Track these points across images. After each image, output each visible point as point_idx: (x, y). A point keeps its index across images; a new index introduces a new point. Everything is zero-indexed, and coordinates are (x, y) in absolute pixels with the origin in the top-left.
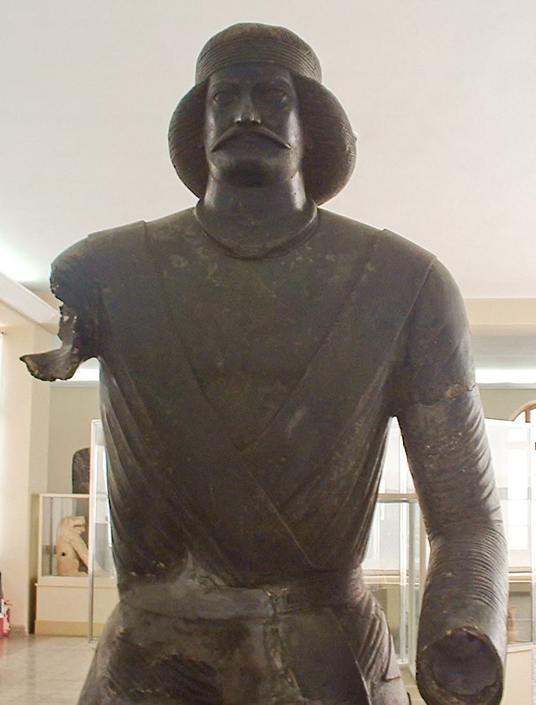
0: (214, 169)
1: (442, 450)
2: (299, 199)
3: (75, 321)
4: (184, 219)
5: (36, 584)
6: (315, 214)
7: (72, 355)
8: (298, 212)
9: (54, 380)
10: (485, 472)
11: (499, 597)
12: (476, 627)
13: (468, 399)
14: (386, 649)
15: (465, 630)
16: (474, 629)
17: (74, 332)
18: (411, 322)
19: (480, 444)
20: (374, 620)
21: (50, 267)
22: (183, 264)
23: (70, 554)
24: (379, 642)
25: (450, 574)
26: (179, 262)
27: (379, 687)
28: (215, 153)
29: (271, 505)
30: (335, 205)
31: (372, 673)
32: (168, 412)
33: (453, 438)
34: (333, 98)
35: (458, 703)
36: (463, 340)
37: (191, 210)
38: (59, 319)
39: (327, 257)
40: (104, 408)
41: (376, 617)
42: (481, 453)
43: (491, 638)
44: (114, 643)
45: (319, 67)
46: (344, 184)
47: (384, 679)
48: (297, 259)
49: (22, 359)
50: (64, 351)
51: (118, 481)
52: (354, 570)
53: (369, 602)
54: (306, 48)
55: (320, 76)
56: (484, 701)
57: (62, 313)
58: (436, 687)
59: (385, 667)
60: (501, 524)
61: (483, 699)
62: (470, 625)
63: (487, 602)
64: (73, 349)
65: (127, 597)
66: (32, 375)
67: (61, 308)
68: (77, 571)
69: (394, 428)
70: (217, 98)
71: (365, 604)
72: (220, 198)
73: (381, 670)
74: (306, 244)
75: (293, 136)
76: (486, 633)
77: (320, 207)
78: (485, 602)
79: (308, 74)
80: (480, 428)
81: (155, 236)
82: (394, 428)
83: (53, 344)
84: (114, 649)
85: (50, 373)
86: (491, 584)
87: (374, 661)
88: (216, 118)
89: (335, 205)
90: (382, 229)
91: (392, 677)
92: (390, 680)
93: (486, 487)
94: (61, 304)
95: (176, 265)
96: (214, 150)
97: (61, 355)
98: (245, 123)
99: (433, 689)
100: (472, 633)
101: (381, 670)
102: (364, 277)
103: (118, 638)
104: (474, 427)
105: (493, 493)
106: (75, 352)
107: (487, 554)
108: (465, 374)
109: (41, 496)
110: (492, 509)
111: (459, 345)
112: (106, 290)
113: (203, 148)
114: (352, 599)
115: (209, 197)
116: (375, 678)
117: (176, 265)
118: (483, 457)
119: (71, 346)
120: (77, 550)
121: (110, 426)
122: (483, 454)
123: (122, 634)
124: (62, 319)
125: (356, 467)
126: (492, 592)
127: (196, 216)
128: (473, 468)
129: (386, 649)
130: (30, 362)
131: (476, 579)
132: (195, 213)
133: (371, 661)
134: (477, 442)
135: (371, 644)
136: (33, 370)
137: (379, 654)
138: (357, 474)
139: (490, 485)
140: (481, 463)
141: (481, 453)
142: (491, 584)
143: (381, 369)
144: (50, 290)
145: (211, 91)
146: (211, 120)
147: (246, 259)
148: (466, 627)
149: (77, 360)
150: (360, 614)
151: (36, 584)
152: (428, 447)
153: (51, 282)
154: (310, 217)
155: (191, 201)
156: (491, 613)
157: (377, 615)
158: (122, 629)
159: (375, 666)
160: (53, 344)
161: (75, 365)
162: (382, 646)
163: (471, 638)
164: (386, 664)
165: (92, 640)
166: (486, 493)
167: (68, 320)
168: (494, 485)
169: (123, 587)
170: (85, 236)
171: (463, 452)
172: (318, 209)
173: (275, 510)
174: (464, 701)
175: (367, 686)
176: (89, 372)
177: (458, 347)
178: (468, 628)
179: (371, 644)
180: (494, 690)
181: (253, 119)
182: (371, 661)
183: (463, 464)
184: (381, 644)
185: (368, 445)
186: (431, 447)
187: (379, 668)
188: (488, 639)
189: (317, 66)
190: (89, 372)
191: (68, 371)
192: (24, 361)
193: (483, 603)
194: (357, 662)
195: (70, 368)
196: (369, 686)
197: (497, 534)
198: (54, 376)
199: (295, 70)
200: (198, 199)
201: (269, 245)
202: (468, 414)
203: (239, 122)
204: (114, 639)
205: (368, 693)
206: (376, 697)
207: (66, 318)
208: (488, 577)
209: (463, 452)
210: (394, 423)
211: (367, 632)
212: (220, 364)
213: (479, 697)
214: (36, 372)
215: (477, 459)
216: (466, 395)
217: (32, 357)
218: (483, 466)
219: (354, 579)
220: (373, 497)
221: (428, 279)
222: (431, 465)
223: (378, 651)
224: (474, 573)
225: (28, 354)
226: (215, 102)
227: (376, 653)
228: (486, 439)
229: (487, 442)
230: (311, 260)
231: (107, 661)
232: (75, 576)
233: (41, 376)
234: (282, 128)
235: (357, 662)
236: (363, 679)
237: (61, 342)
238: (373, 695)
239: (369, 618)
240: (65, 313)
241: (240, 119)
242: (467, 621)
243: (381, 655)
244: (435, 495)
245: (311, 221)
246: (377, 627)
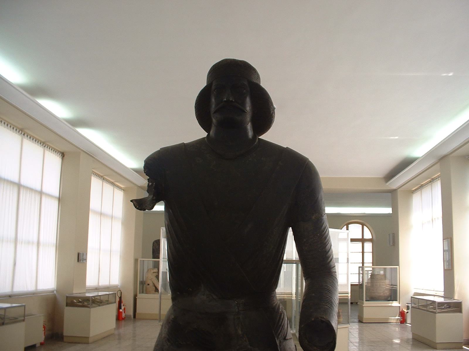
0: (214, 120)
2: (250, 134)
3: (154, 185)
4: (201, 142)
5: (137, 297)
6: (257, 140)
7: (153, 200)
9: (145, 210)
10: (329, 251)
11: (335, 304)
12: (325, 317)
14: (286, 326)
15: (320, 318)
16: (324, 318)
17: (154, 190)
19: (327, 239)
20: (281, 314)
21: (144, 162)
23: (151, 284)
24: (283, 322)
25: (314, 294)
30: (266, 137)
31: (280, 336)
37: (204, 138)
38: (147, 184)
40: (166, 222)
41: (282, 312)
42: (327, 244)
43: (331, 322)
44: (170, 322)
45: (260, 77)
47: (285, 339)
49: (131, 201)
50: (150, 198)
52: (273, 293)
53: (279, 306)
55: (260, 81)
57: (148, 182)
59: (285, 334)
60: (336, 273)
62: (322, 316)
63: (329, 306)
64: (153, 197)
66: (136, 208)
67: (148, 179)
68: (154, 292)
69: (290, 233)
70: (216, 91)
71: (277, 307)
73: (284, 335)
75: (248, 108)
77: (259, 137)
78: (328, 306)
82: (290, 233)
83: (145, 195)
85: (143, 207)
86: (331, 299)
87: (281, 331)
88: (215, 99)
89: (266, 137)
90: (286, 147)
91: (289, 338)
92: (288, 339)
94: (148, 178)
96: (214, 113)
97: (148, 199)
98: (228, 101)
100: (323, 319)
101: (284, 335)
104: (324, 232)
105: (332, 260)
106: (154, 198)
107: (330, 286)
108: (321, 209)
109: (139, 259)
110: (332, 267)
111: (318, 197)
115: (211, 133)
116: (281, 338)
118: (328, 245)
119: (152, 196)
120: (154, 282)
121: (169, 230)
122: (328, 243)
123: (173, 319)
124: (148, 184)
126: (332, 302)
127: (207, 141)
128: (324, 249)
129: (286, 326)
130: (135, 202)
131: (325, 297)
133: (279, 331)
134: (326, 238)
135: (279, 324)
137: (283, 328)
139: (331, 256)
140: (327, 247)
141: (327, 244)
142: (331, 299)
144: (144, 171)
145: (213, 87)
146: (213, 100)
148: (320, 317)
151: (137, 297)
152: (305, 240)
153: (144, 168)
154: (255, 142)
155: (204, 134)
157: (282, 312)
158: (173, 317)
159: (281, 333)
160: (145, 195)
161: (154, 204)
162: (284, 325)
163: (322, 322)
164: (286, 332)
165: (160, 321)
167: (152, 184)
168: (333, 256)
169: (174, 299)
170: (159, 149)
172: (259, 138)
175: (278, 342)
176: (160, 207)
177: (318, 198)
178: (321, 317)
179: (279, 324)
181: (231, 100)
182: (279, 331)
184: (284, 324)
187: (283, 334)
188: (330, 322)
189: (258, 77)
190: (160, 207)
192: (132, 202)
193: (328, 307)
194: (273, 332)
195: (152, 205)
196: (279, 342)
197: (334, 278)
200: (207, 134)
202: (322, 226)
203: (225, 101)
204: (170, 321)
205: (278, 345)
206: (281, 347)
207: (150, 184)
208: (330, 296)
211: (278, 319)
214: (137, 207)
216: (321, 218)
217: (136, 200)
218: (328, 248)
219: (273, 296)
222: (306, 248)
223: (283, 326)
224: (324, 294)
225: (134, 199)
226: (215, 92)
227: (282, 328)
228: (330, 237)
229: (330, 238)
231: (167, 330)
232: (153, 294)
233: (140, 208)
234: (243, 104)
235: (273, 332)
236: (276, 339)
237: (148, 194)
238: (280, 346)
240: (150, 182)
241: (225, 100)
243: (284, 329)
245: (255, 143)
246: (282, 317)
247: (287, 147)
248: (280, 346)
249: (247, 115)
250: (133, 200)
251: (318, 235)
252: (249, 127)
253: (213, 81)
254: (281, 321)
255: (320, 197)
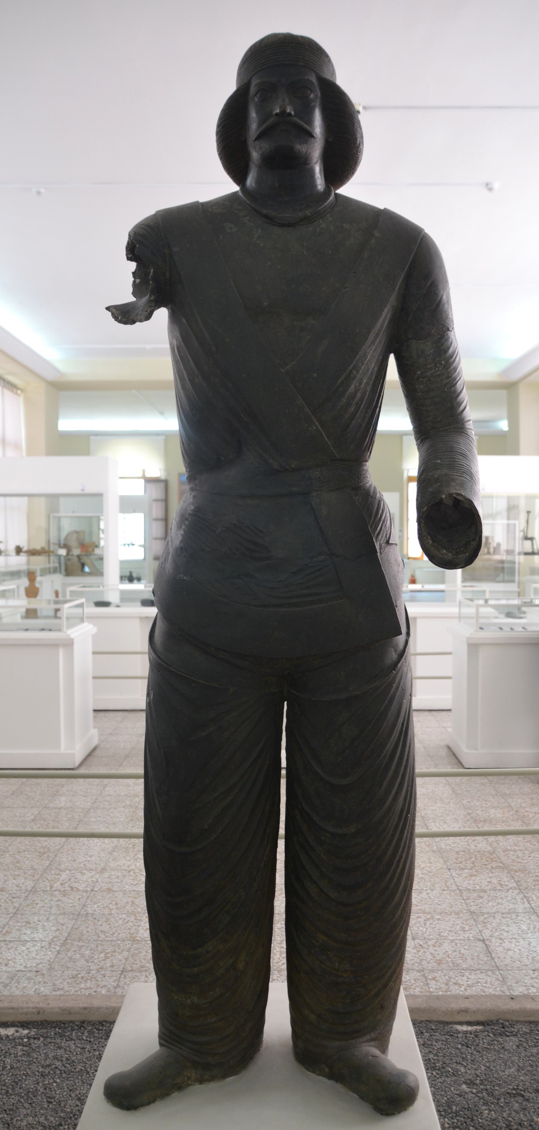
0: (255, 155)
1: (430, 374)
8: (318, 193)
9: (133, 322)
12: (463, 494)
13: (449, 338)
15: (455, 496)
16: (461, 495)
18: (408, 277)
20: (379, 502)
22: (234, 230)
26: (231, 228)
27: (385, 548)
28: (257, 142)
29: (307, 409)
30: (347, 190)
31: (380, 537)
32: (228, 340)
33: (438, 365)
34: (349, 98)
35: (447, 555)
36: (445, 293)
37: (236, 193)
39: (344, 225)
42: (458, 378)
44: (187, 519)
46: (353, 173)
47: (388, 542)
48: (322, 226)
49: (108, 309)
51: (188, 397)
54: (327, 56)
56: (466, 553)
57: (134, 277)
58: (430, 542)
59: (389, 534)
61: (465, 551)
62: (459, 492)
64: (150, 297)
65: (196, 485)
66: (116, 320)
70: (258, 95)
72: (259, 181)
73: (386, 536)
74: (328, 215)
76: (470, 498)
79: (328, 76)
80: (457, 359)
81: (210, 210)
84: (187, 523)
85: (131, 318)
88: (257, 113)
90: (382, 208)
92: (392, 544)
93: (461, 405)
95: (229, 231)
96: (258, 138)
98: (283, 113)
99: (428, 543)
100: (459, 498)
101: (386, 536)
102: (373, 241)
103: (189, 514)
106: (152, 298)
111: (442, 296)
112: (175, 249)
113: (245, 142)
114: (364, 484)
115: (250, 181)
117: (229, 231)
121: (180, 356)
123: (192, 510)
124: (134, 282)
125: (367, 383)
126: (472, 473)
130: (114, 310)
132: (240, 194)
133: (379, 528)
134: (455, 369)
136: (117, 316)
138: (369, 389)
139: (465, 402)
140: (458, 385)
141: (458, 378)
143: (386, 310)
146: (253, 115)
147: (283, 225)
149: (153, 304)
150: (370, 495)
154: (328, 198)
155: (234, 188)
156: (472, 486)
158: (192, 508)
159: (382, 532)
161: (153, 308)
164: (389, 532)
166: (462, 408)
167: (140, 282)
171: (445, 376)
173: (310, 413)
174: (451, 552)
175: (377, 547)
176: (162, 314)
180: (474, 543)
181: (288, 111)
182: (379, 528)
183: (446, 385)
184: (385, 517)
185: (376, 368)
186: (421, 373)
187: (385, 535)
190: (162, 314)
191: (146, 313)
195: (149, 310)
198: (135, 318)
199: (320, 73)
201: (301, 214)
202: (449, 348)
203: (277, 114)
204: (187, 516)
205: (378, 551)
206: (383, 555)
207: (138, 281)
209: (445, 376)
210: (392, 360)
212: (266, 304)
213: (462, 549)
215: (455, 382)
216: (447, 334)
217: (115, 307)
218: (460, 386)
220: (378, 409)
221: (420, 244)
222: (421, 386)
224: (457, 460)
230: (332, 227)
231: (182, 532)
233: (124, 320)
234: (310, 121)
238: (381, 553)
239: (376, 498)
241: (278, 111)
242: (456, 489)
243: (386, 525)
244: (424, 408)
245: (331, 198)
246: (382, 505)
247: (385, 209)
248: (381, 553)
249: (316, 145)
250: (111, 306)
251: (443, 363)
252: (317, 169)
253: (252, 76)
254: (381, 511)
255: (444, 297)
